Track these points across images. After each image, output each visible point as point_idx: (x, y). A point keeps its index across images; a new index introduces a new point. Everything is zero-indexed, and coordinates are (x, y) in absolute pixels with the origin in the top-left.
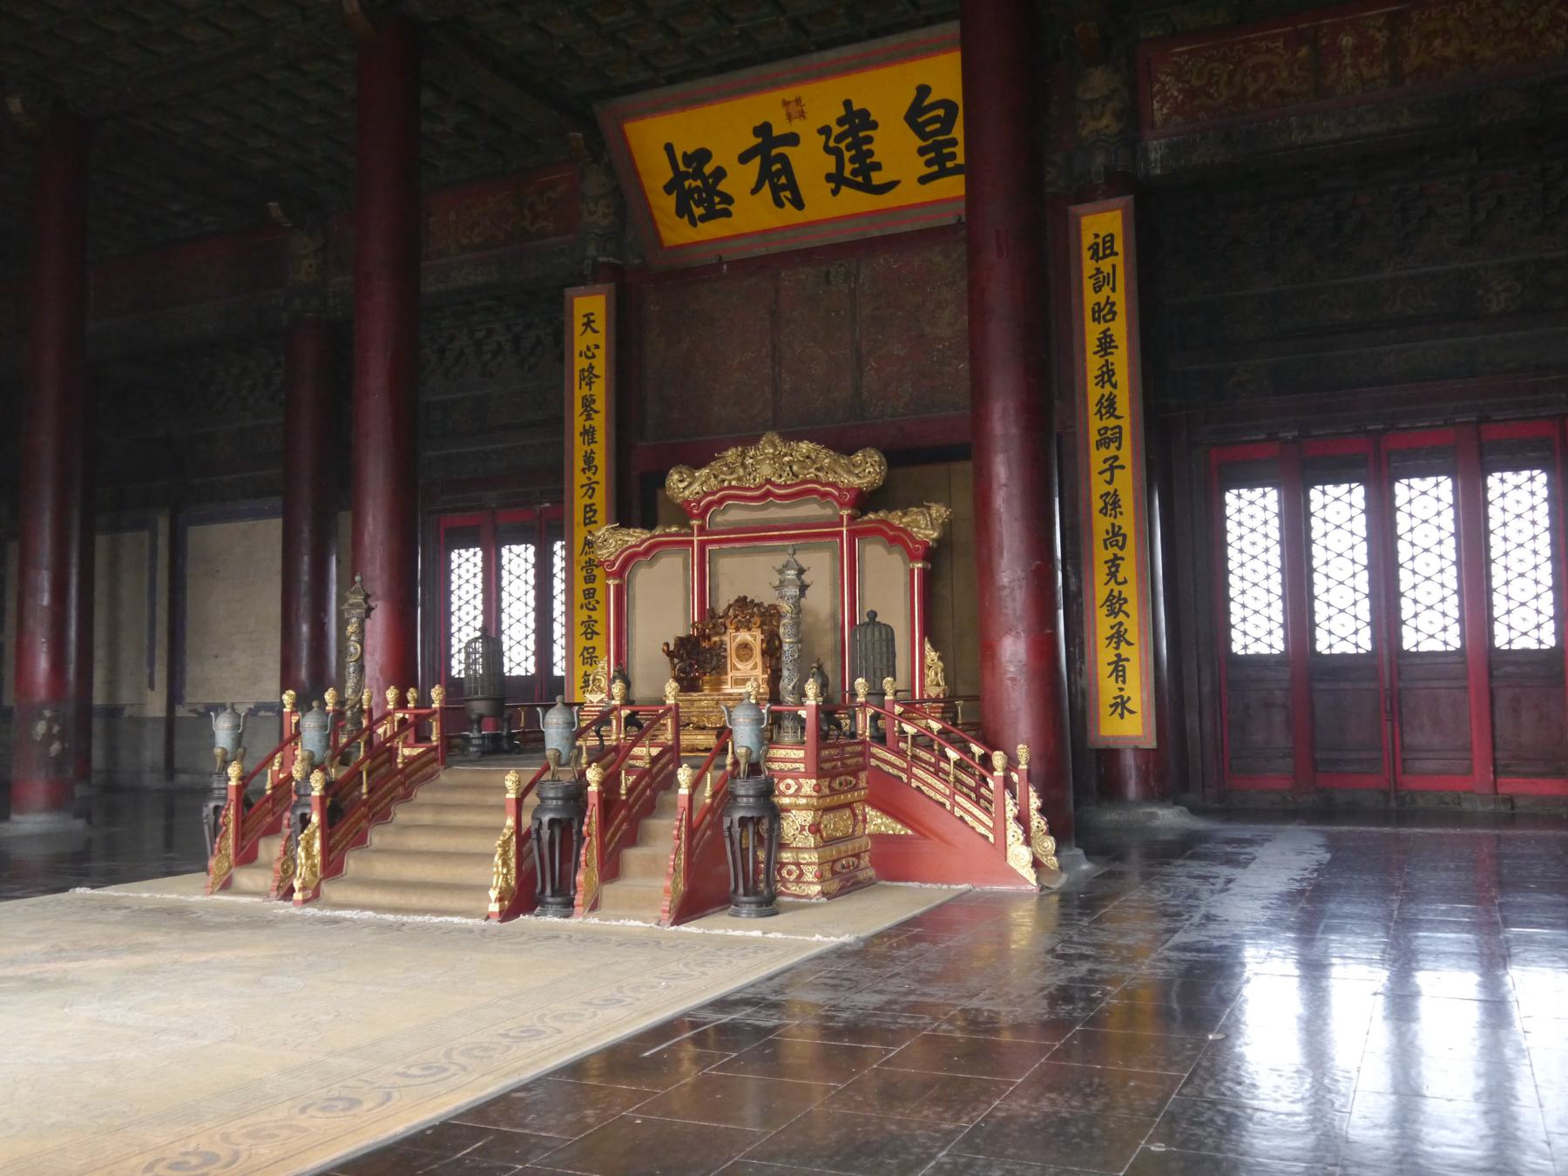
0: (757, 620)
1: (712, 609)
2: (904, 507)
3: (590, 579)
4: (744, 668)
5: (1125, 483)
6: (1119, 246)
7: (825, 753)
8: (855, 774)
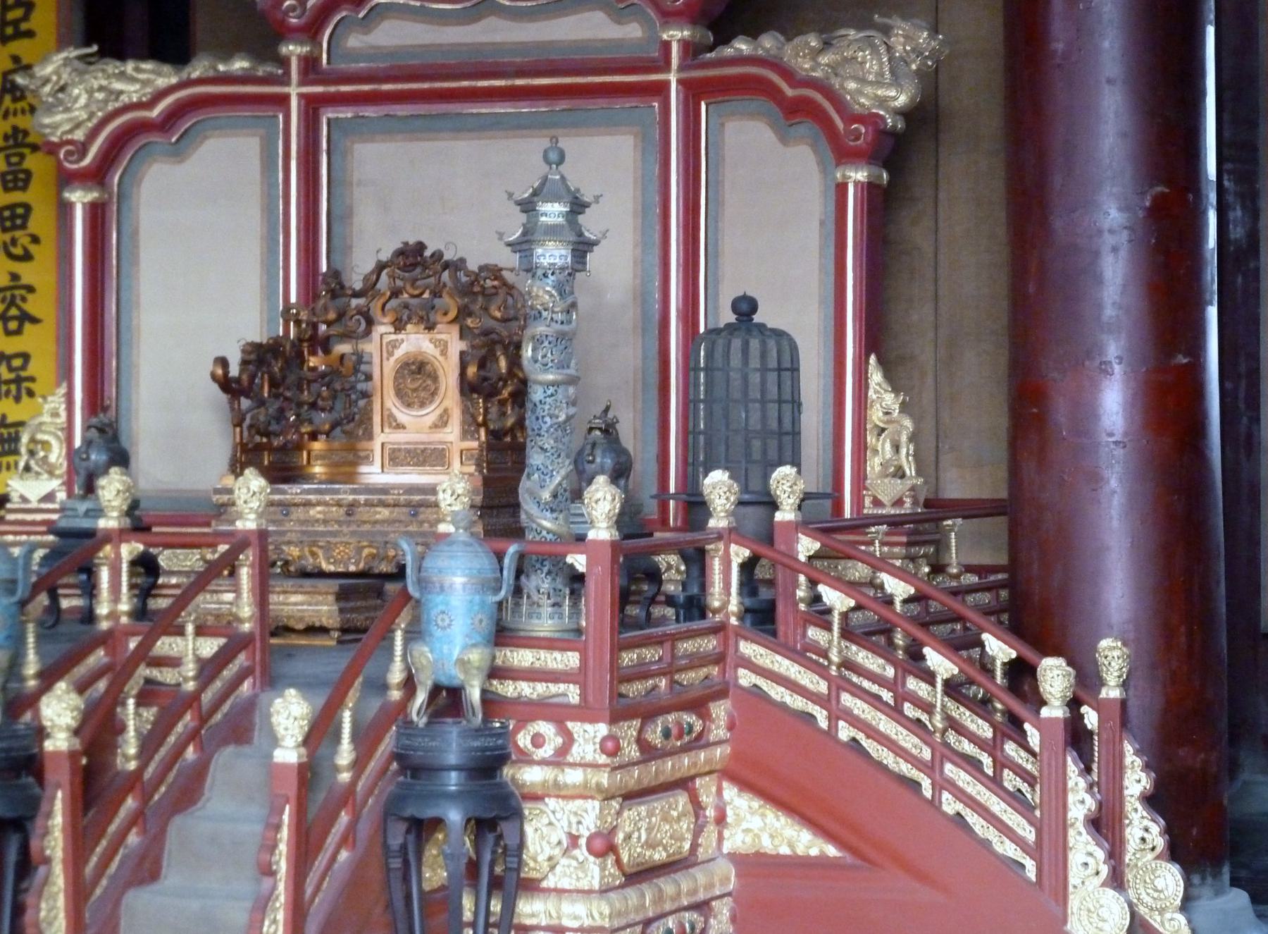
0: (450, 303)
1: (335, 274)
2: (827, 29)
7: (628, 658)
8: (699, 705)
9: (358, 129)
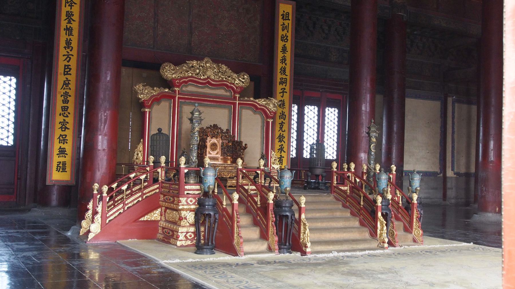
3: (66, 101)
4: (214, 154)
5: (287, 97)
6: (290, 18)
9: (184, 103)
